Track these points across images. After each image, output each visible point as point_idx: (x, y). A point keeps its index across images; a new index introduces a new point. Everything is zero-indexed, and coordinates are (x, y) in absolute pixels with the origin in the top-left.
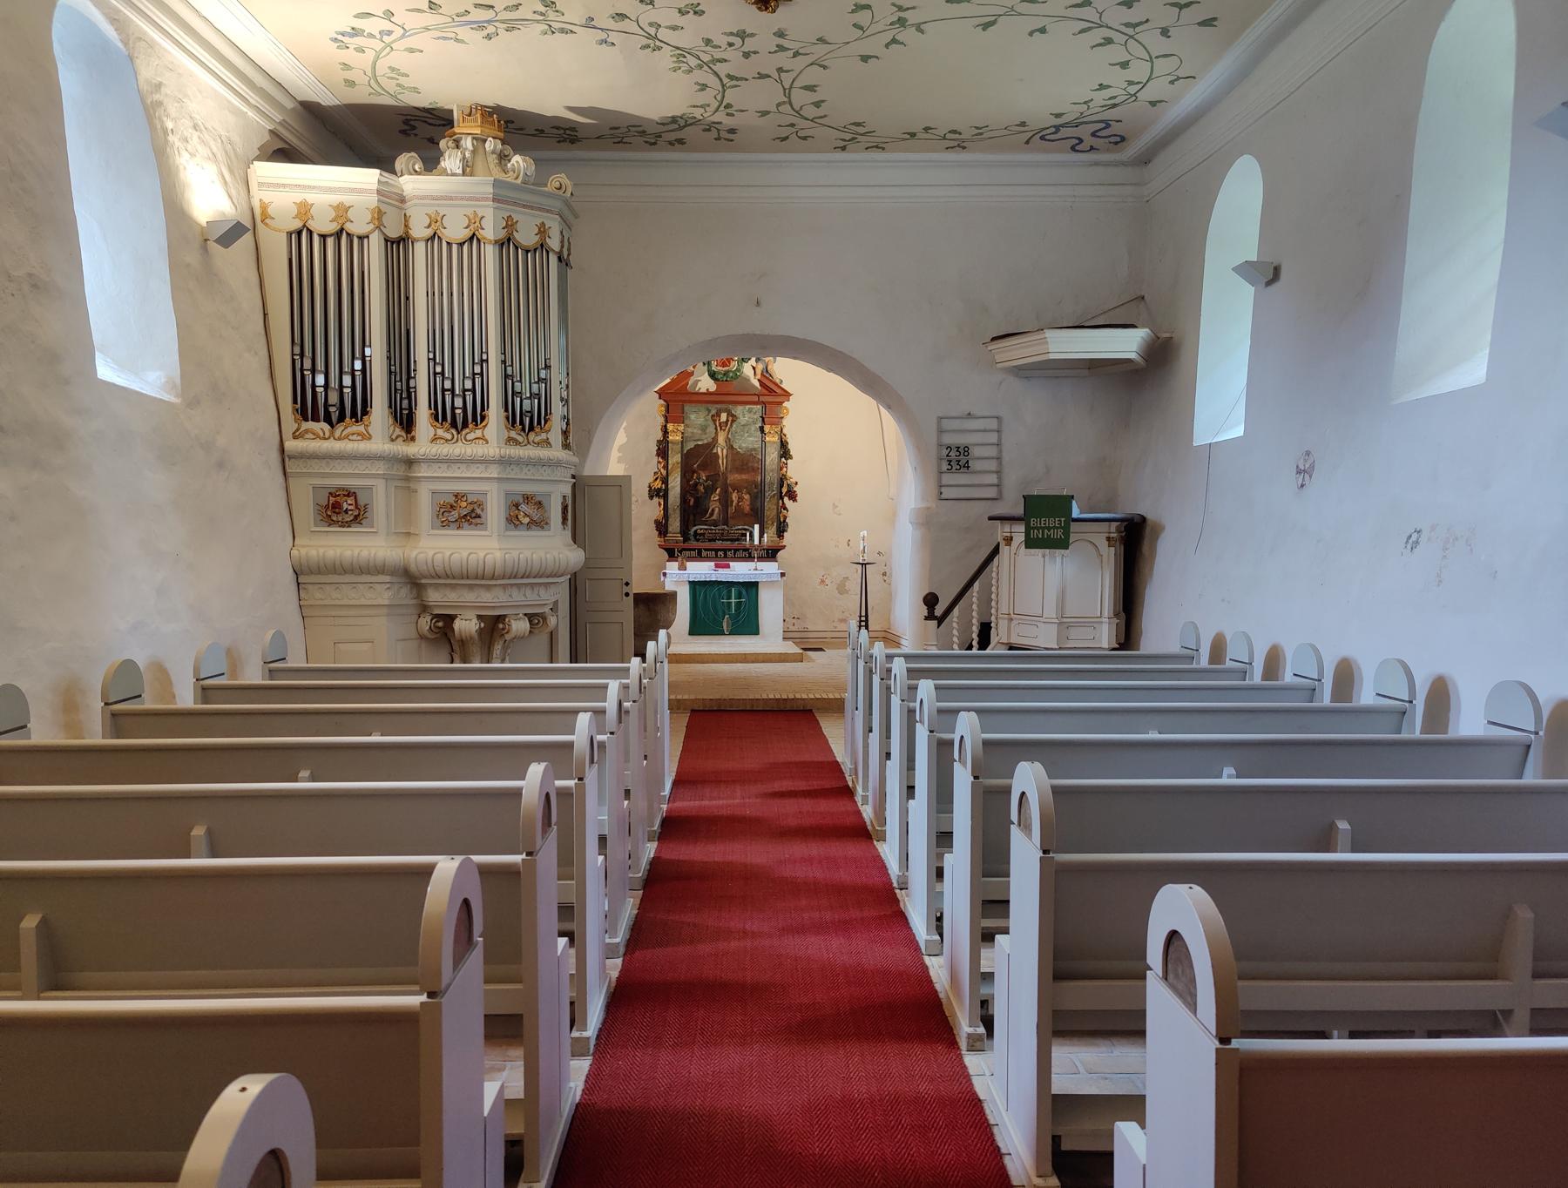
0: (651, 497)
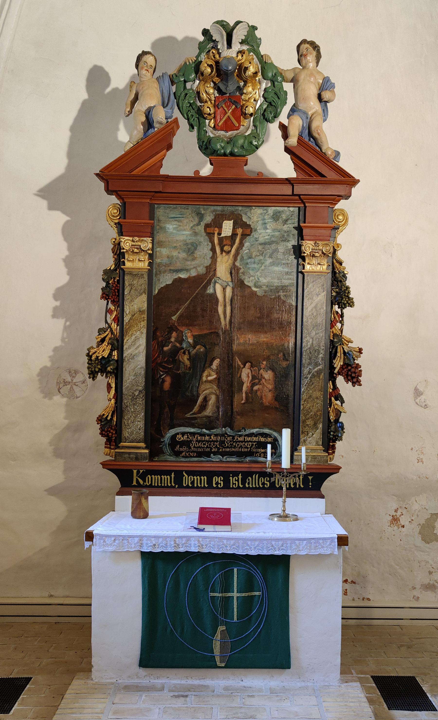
0: (93, 375)
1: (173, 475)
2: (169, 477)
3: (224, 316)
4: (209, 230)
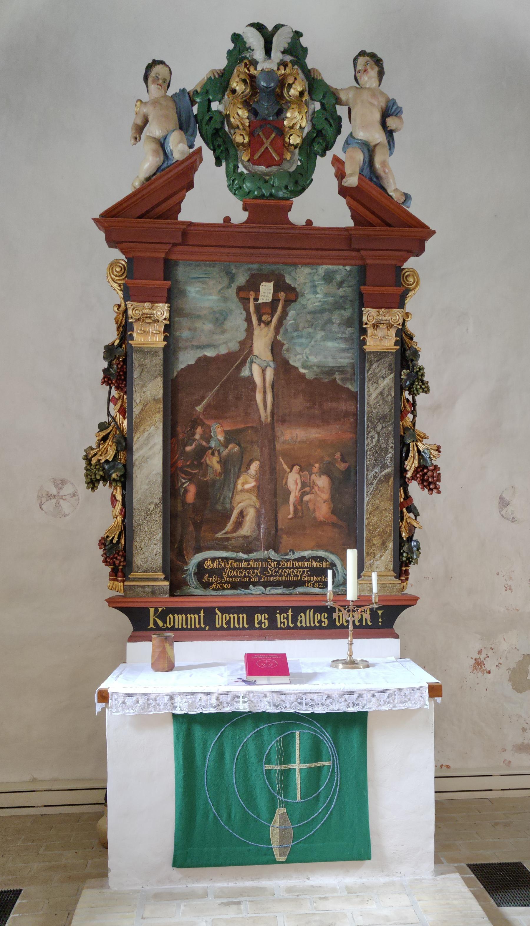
0: (92, 484)
1: (202, 614)
2: (196, 616)
3: (264, 405)
4: (243, 294)
